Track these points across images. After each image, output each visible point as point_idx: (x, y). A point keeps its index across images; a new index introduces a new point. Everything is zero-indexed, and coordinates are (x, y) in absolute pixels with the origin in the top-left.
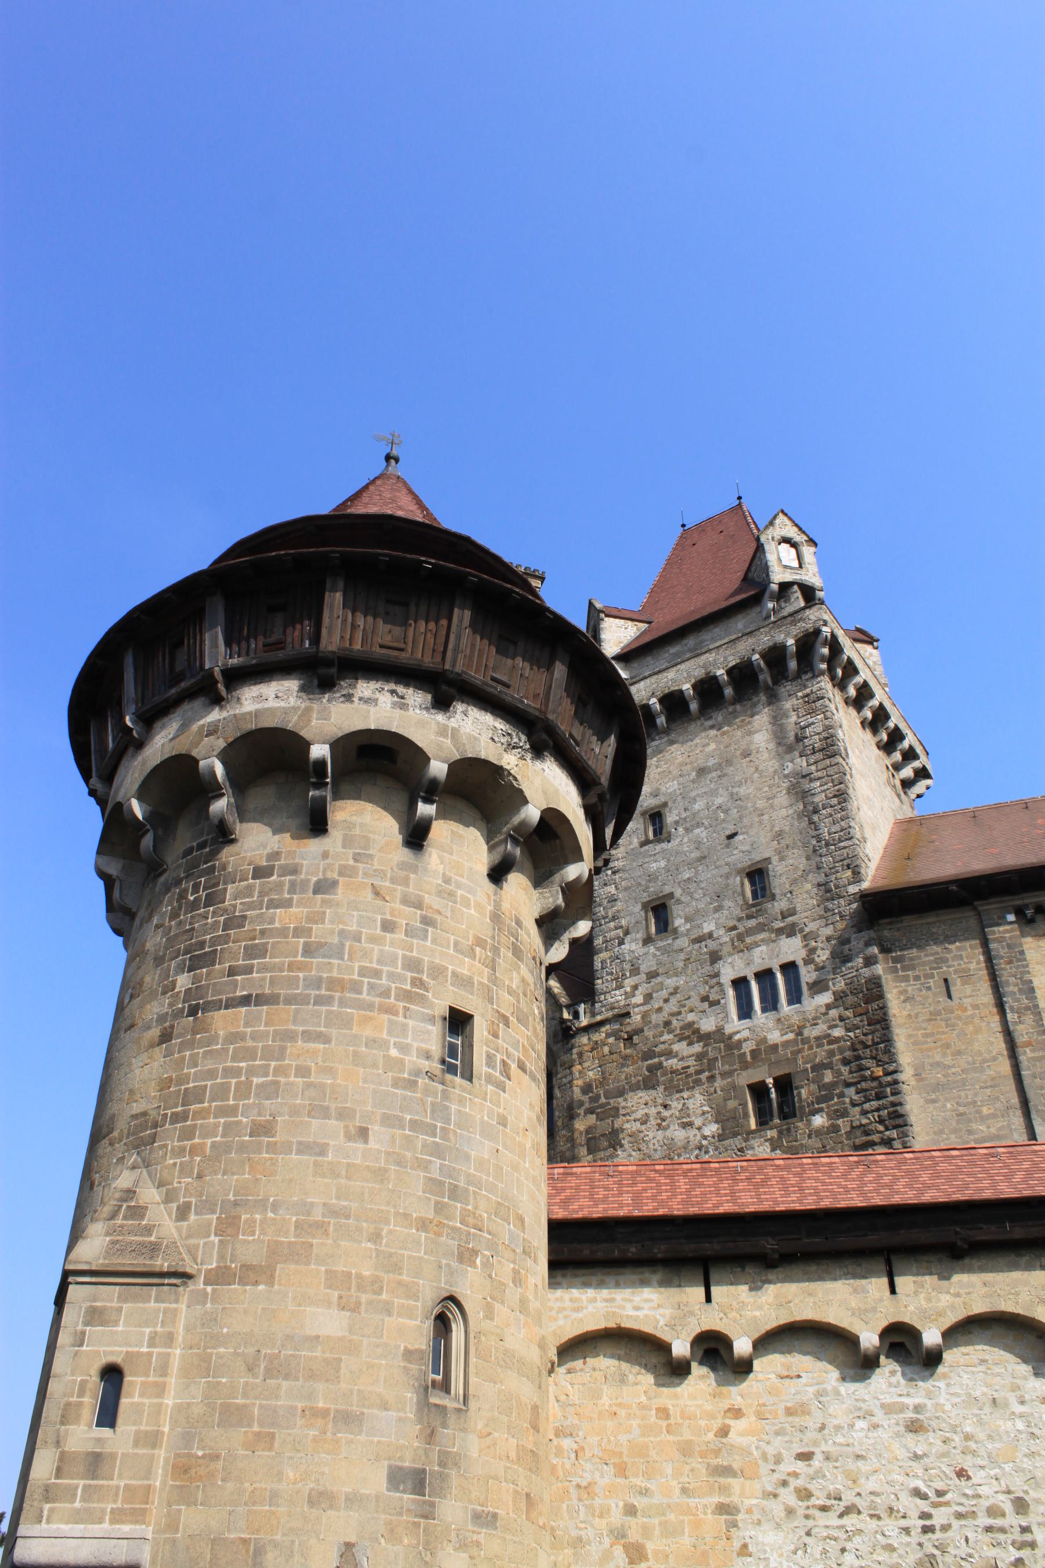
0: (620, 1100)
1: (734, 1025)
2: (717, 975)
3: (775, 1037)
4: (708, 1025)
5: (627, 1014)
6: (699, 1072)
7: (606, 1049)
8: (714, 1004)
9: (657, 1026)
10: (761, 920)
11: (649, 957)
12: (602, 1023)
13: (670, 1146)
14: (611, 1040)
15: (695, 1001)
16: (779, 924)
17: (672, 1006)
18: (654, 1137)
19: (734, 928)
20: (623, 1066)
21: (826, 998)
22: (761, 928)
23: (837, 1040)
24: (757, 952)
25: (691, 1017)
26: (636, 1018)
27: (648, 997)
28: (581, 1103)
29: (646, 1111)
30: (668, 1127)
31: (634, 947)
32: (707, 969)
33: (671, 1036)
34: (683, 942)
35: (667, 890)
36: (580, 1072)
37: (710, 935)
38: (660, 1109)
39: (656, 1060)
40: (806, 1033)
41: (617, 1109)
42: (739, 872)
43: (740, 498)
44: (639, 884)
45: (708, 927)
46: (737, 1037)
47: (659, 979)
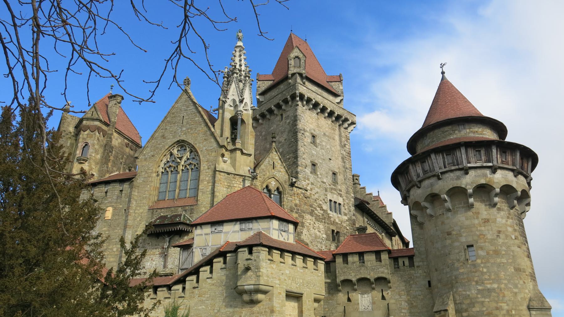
0: (304, 214)
1: (329, 212)
2: (326, 195)
3: (337, 220)
4: (325, 207)
5: (307, 191)
6: (322, 219)
7: (301, 197)
8: (326, 203)
9: (313, 199)
10: (335, 187)
11: (312, 177)
12: (300, 188)
13: (316, 234)
14: (302, 195)
15: (321, 199)
16: (338, 192)
17: (316, 196)
18: (312, 231)
19: (330, 185)
20: (305, 205)
21: (346, 218)
22: (335, 190)
23: (347, 229)
24: (335, 196)
25: (321, 202)
26: (308, 193)
27: (311, 190)
28: (294, 209)
29: (310, 221)
30: (315, 229)
31: (308, 172)
32: (324, 191)
33: (316, 204)
34: (319, 180)
35: (316, 162)
36: (294, 199)
37: (325, 183)
38: (313, 223)
39: (313, 209)
40: (343, 223)
41: (304, 217)
42: (332, 171)
43: (306, 40)
44: (310, 154)
45: (325, 181)
46: (330, 215)
47: (314, 186)
